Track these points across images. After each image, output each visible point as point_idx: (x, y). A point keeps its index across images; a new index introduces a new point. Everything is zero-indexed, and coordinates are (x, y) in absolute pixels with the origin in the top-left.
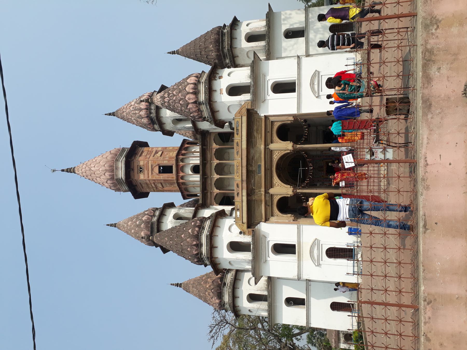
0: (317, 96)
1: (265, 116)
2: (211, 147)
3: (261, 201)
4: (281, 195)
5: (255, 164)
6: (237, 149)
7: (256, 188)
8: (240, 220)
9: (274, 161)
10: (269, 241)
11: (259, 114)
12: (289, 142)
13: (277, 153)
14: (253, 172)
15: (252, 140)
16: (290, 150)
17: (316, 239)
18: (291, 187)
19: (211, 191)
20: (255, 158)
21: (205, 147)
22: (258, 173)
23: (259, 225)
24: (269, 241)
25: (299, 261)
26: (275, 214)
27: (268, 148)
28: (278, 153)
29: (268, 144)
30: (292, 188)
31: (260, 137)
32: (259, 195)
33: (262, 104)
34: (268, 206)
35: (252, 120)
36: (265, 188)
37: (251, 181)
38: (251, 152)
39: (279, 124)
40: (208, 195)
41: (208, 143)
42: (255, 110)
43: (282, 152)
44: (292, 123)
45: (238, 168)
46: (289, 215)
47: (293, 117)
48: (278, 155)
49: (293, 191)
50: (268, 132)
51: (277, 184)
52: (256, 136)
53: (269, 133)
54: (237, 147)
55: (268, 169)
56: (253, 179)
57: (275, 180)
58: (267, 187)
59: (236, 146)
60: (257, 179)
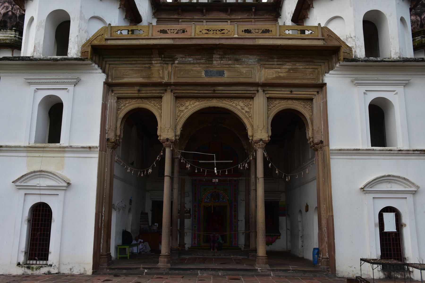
0: (365, 189)
1: (325, 84)
2: (253, 20)
3: (149, 77)
4: (161, 116)
5: (224, 66)
6: (257, 31)
7: (176, 67)
8: (111, 36)
9: (231, 103)
10: (68, 92)
11: (328, 73)
12: (270, 134)
13: (246, 109)
14: (210, 60)
15: (276, 60)
16: (252, 136)
17: (69, 184)
18: (177, 138)
19: (180, 20)
20: (238, 66)
21: (254, 10)
22: (206, 72)
23: (100, 71)
24: (68, 92)
25: (25, 149)
26: (122, 105)
27: (258, 91)
28: (246, 112)
29: (266, 92)
30: (173, 138)
31: (282, 75)
32: (161, 73)
33: (349, 80)
34: (139, 91)
35: (315, 61)
36: (176, 84)
37: (190, 55)
38: (251, 57)
39: (307, 115)
40: (174, 16)
41: (261, 15)
42: (337, 65)
43: (250, 119)
44: (307, 140)
45: (218, 32)
46: (118, 133)
47: (322, 142)
48: (244, 111)
49: (167, 140)
50: (291, 91)
51: (183, 108)
52: (284, 67)
53: (289, 92)
54: (260, 31)
55: (214, 90)
56: (194, 60)
57: (193, 106)
58: (178, 88)
59: (263, 29)
60: (194, 69)
